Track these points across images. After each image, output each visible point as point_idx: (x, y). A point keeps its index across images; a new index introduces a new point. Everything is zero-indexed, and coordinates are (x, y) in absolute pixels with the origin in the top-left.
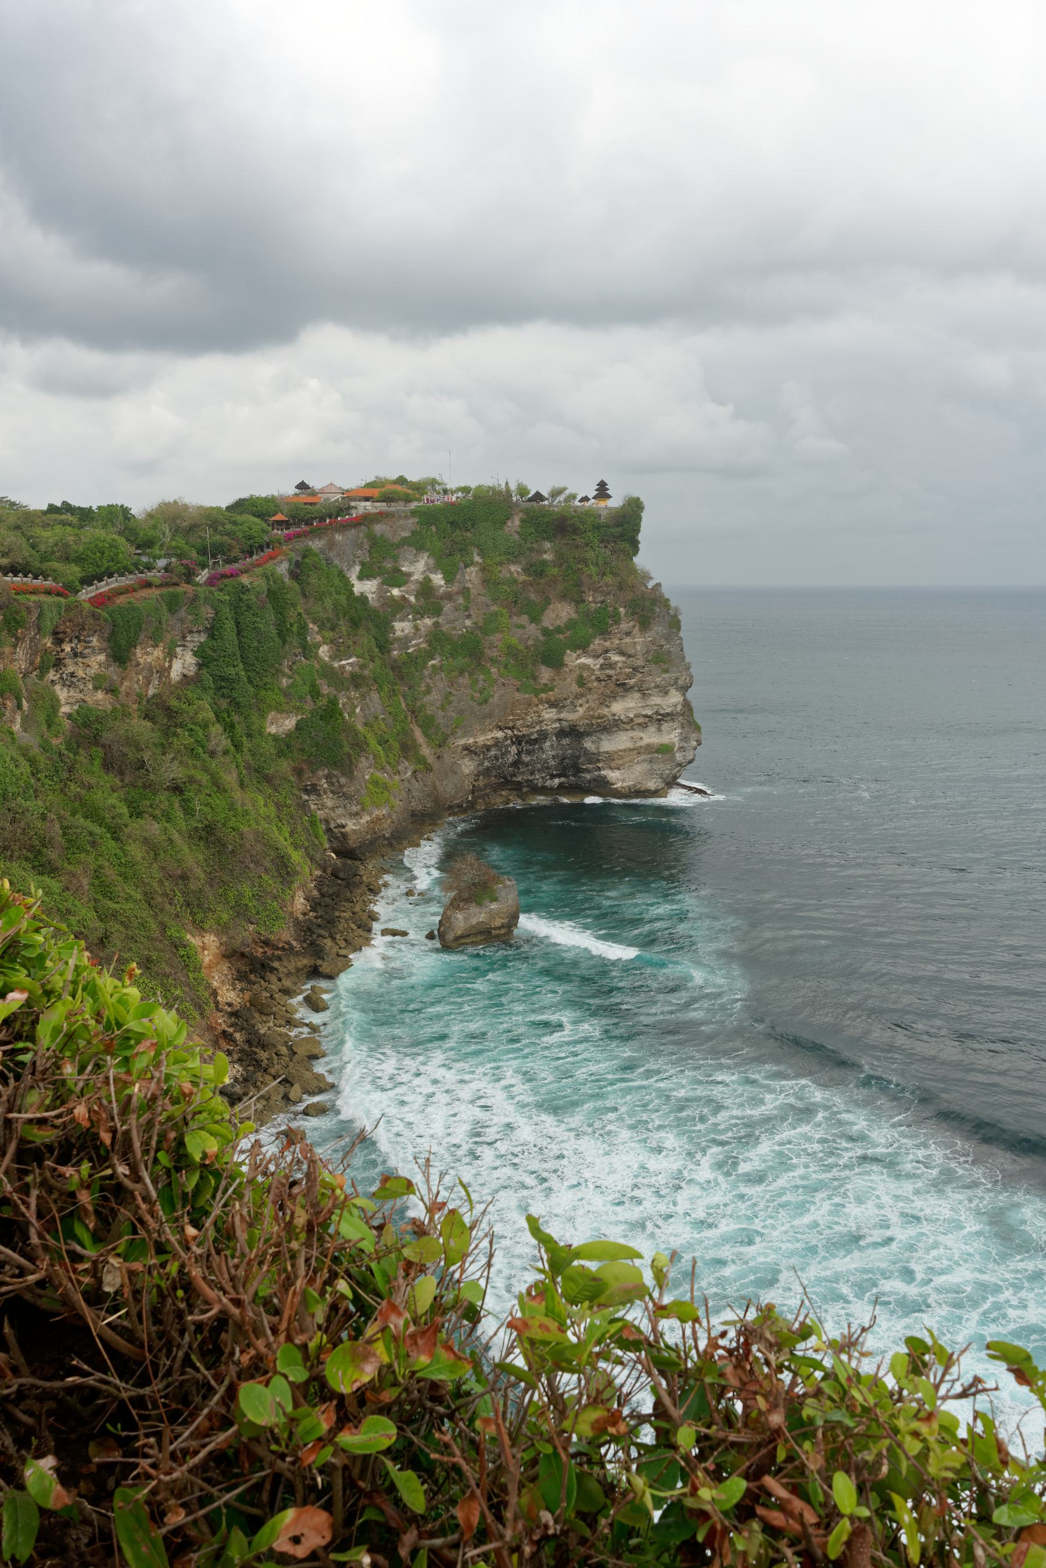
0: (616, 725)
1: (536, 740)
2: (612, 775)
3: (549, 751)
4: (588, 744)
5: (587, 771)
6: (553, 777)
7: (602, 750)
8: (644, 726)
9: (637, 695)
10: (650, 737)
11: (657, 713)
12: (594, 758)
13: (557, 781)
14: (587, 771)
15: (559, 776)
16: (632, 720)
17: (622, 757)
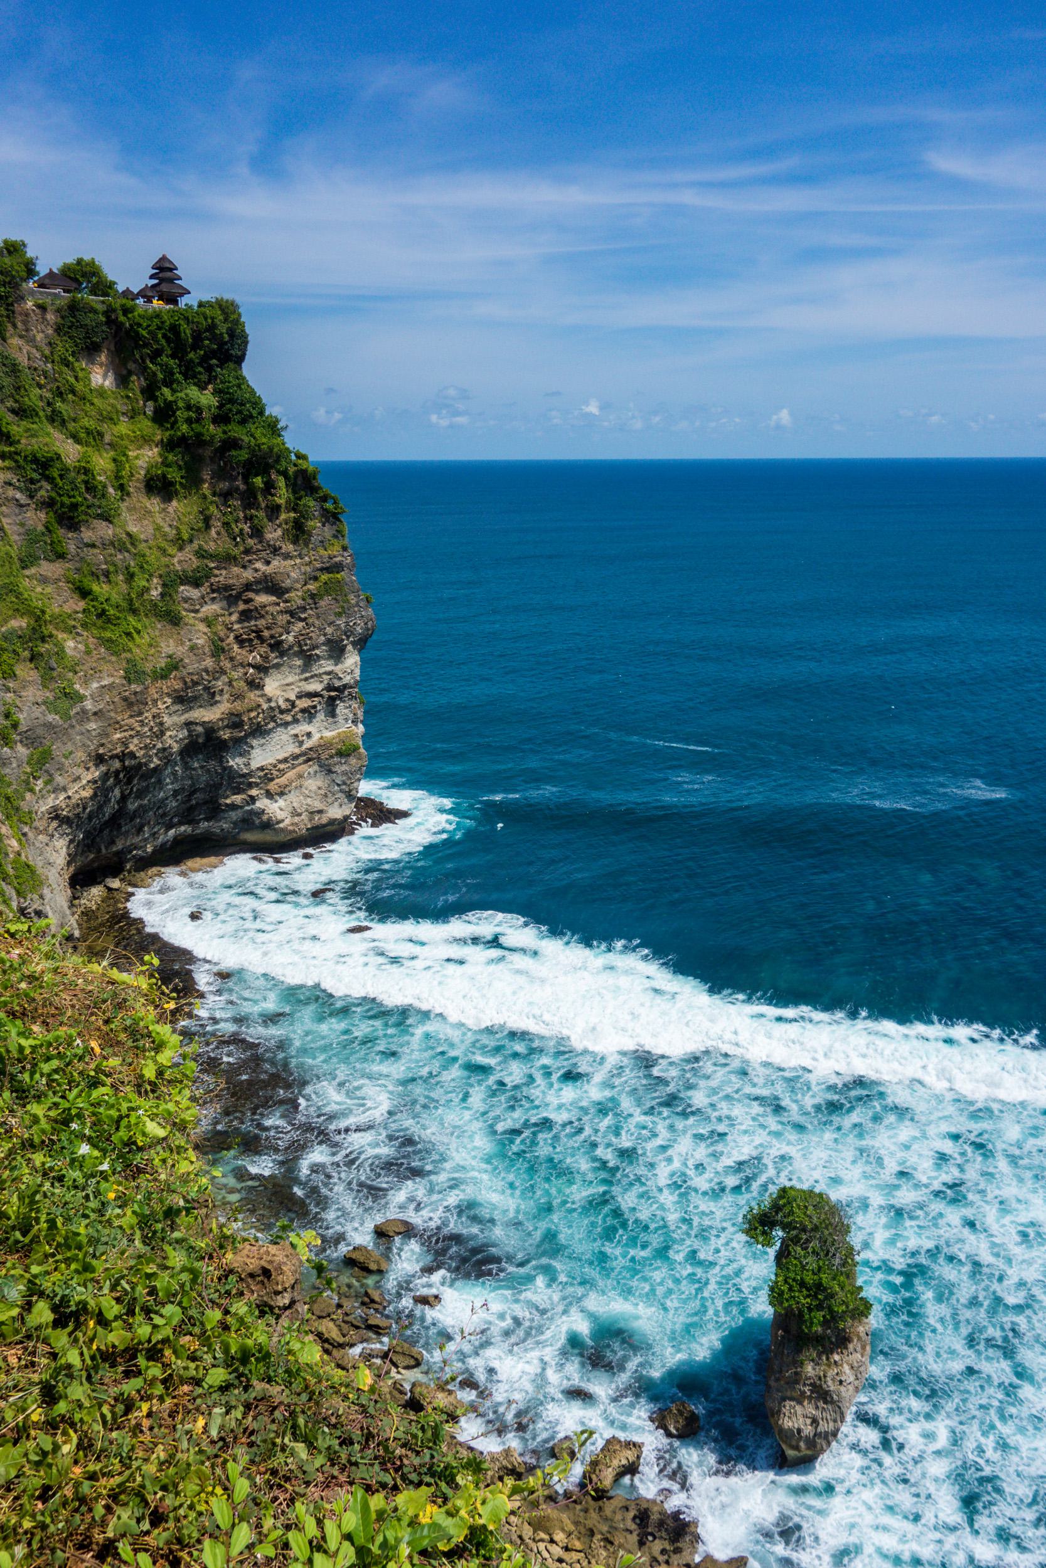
0: (273, 719)
2: (276, 809)
4: (235, 762)
5: (233, 807)
6: (170, 827)
8: (309, 714)
10: (319, 731)
11: (330, 688)
12: (240, 782)
17: (282, 772)
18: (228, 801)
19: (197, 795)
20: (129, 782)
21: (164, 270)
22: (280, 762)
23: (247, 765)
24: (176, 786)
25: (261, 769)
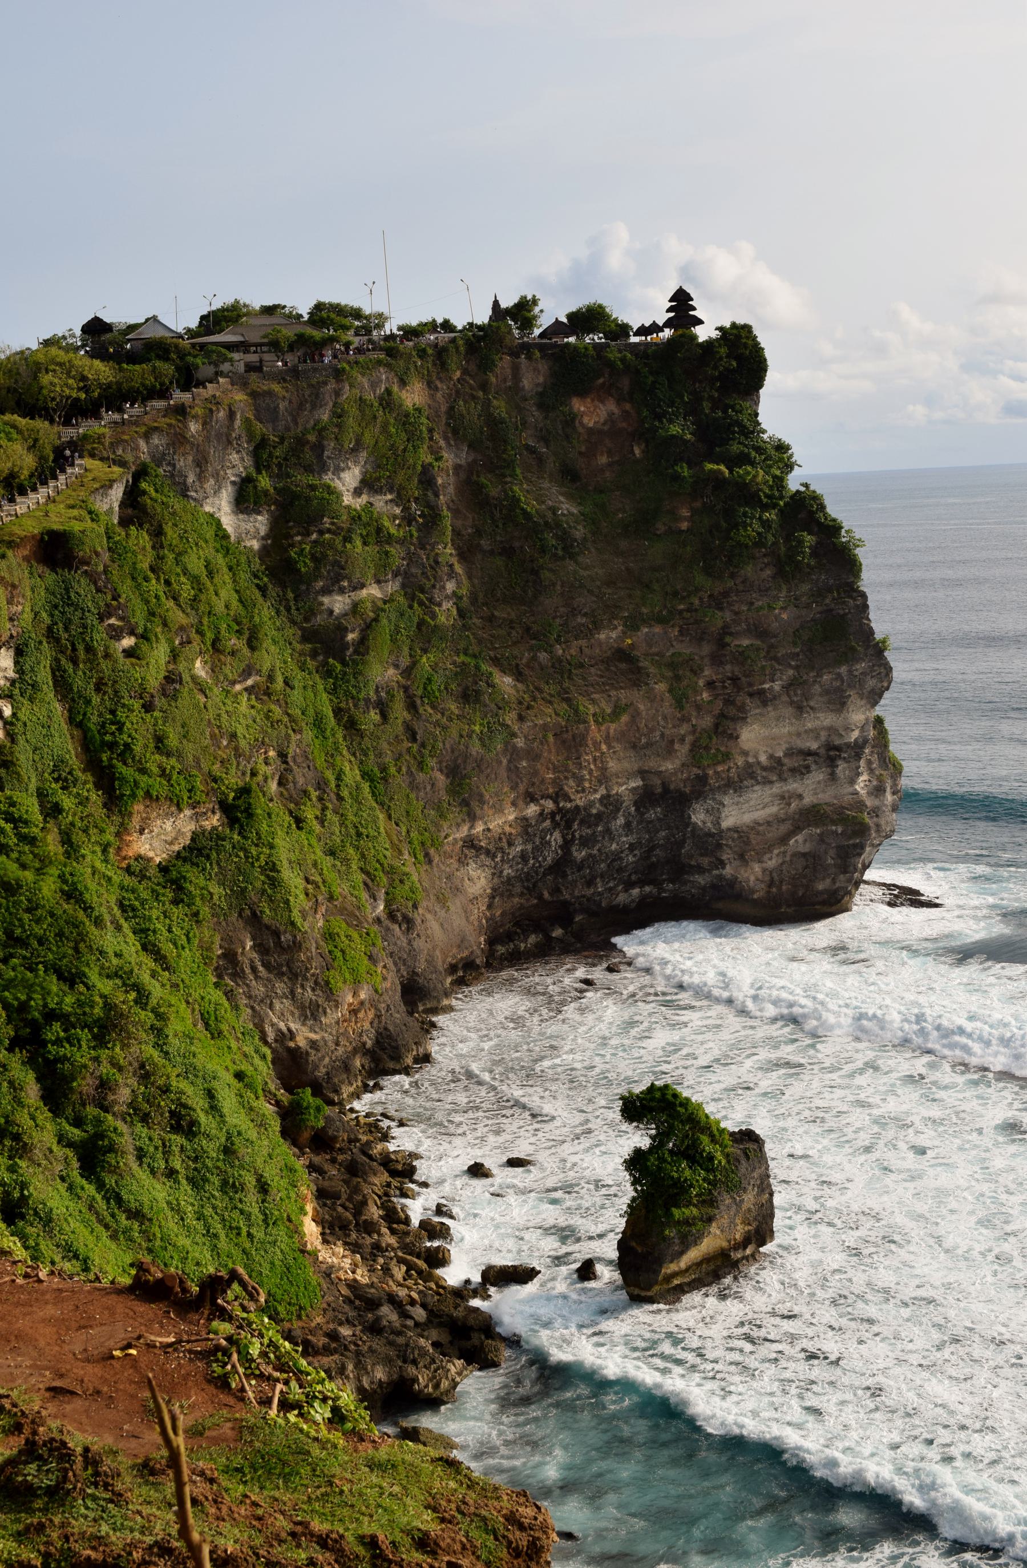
0: (752, 776)
1: (599, 816)
3: (620, 841)
6: (629, 885)
7: (725, 824)
8: (801, 772)
9: (788, 711)
11: (830, 747)
12: (711, 843)
13: (636, 892)
14: (700, 870)
15: (641, 883)
16: (779, 761)
18: (693, 863)
19: (657, 852)
20: (568, 825)
21: (681, 300)
22: (757, 823)
23: (717, 823)
24: (631, 839)
25: (735, 829)
